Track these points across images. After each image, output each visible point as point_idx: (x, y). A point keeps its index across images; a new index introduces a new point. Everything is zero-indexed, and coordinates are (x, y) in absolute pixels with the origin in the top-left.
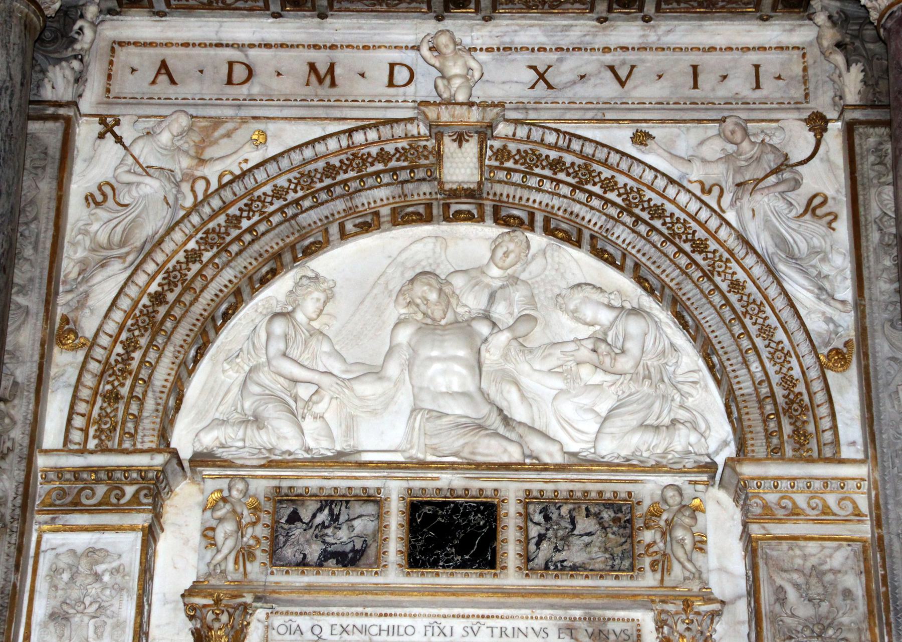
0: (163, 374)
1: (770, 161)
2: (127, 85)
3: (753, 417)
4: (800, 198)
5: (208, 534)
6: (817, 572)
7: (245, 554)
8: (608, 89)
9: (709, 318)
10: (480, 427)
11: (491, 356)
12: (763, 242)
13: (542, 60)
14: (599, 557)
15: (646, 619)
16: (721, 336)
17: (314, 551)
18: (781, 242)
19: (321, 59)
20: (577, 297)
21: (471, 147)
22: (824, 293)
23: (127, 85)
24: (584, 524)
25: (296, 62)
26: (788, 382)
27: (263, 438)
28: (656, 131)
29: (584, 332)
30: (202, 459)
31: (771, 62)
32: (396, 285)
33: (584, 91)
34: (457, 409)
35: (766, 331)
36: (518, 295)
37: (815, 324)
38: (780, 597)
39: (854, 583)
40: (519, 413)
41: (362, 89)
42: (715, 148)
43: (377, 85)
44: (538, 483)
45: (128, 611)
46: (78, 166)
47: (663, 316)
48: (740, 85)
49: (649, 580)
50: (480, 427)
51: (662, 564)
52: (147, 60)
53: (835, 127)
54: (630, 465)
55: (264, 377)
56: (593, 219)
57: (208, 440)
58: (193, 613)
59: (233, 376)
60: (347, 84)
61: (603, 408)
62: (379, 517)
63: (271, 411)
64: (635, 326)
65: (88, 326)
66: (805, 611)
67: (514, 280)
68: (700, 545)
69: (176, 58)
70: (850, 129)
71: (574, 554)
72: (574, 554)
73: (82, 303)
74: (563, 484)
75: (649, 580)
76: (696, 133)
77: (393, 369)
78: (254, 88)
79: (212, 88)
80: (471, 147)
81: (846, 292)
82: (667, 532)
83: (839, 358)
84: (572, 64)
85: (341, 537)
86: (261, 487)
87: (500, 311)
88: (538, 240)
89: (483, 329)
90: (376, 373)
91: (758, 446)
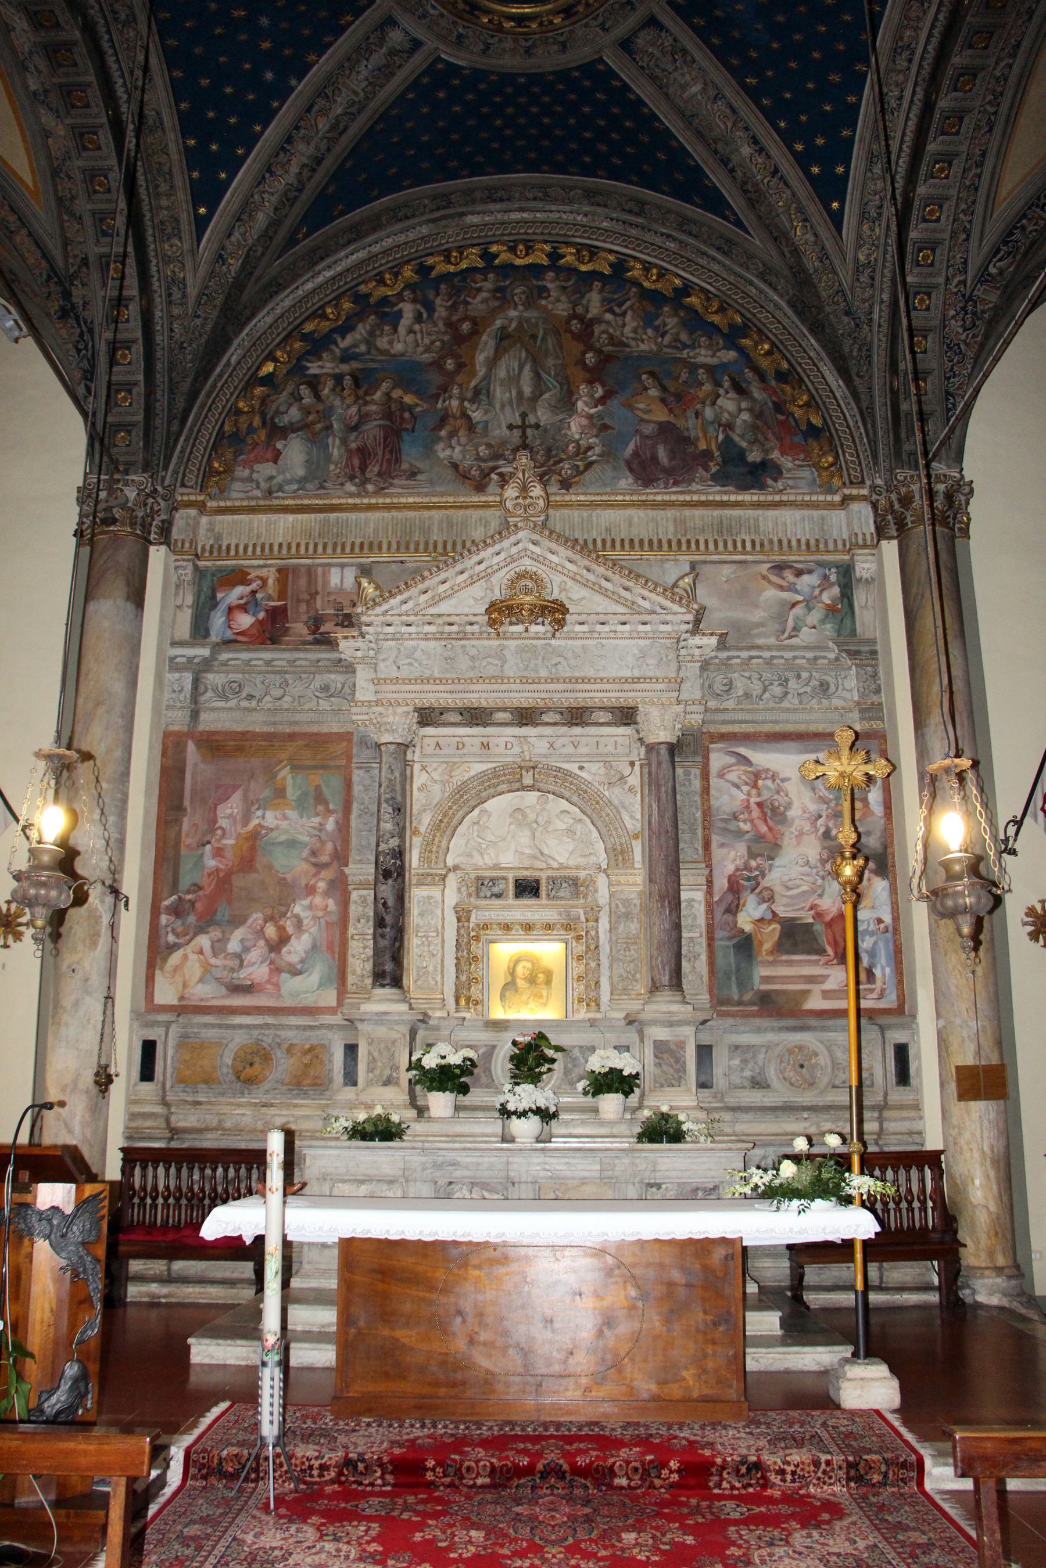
0: (444, 845)
1: (618, 777)
2: (428, 750)
3: (612, 855)
4: (627, 787)
5: (459, 889)
6: (627, 900)
7: (470, 895)
8: (571, 749)
9: (599, 824)
10: (535, 857)
11: (537, 834)
12: (616, 802)
13: (551, 740)
14: (568, 895)
15: (581, 911)
16: (603, 830)
17: (489, 894)
18: (621, 802)
19: (485, 740)
20: (562, 816)
21: (531, 773)
22: (632, 817)
23: (428, 750)
24: (564, 885)
25: (477, 741)
26: (621, 844)
27: (474, 861)
28: (585, 765)
29: (564, 826)
30: (456, 868)
31: (620, 740)
32: (510, 811)
33: (565, 751)
34: (528, 851)
35: (616, 829)
36: (545, 814)
37: (629, 827)
38: (617, 906)
39: (637, 902)
40: (546, 851)
41: (498, 750)
42: (603, 771)
43: (501, 750)
44: (550, 873)
45: (439, 913)
46: (415, 779)
47: (588, 821)
48: (610, 748)
49: (582, 901)
50: (535, 857)
51: (585, 897)
52: (432, 742)
53: (637, 763)
54: (577, 868)
55: (472, 842)
56: (567, 794)
57: (457, 861)
58: (457, 912)
59: (463, 841)
60: (493, 749)
61: (571, 849)
62: (507, 883)
63: (475, 853)
64: (579, 826)
65: (422, 829)
66: (623, 910)
67: (544, 809)
68: (596, 891)
69: (441, 741)
70: (641, 766)
71: (561, 894)
72: (561, 894)
73: (419, 823)
74: (557, 874)
75: (582, 901)
76: (598, 765)
77: (509, 838)
78: (465, 751)
79: (452, 751)
80: (531, 773)
81: (639, 817)
82: (587, 887)
83: (636, 837)
84: (560, 741)
85: (496, 890)
86: (473, 876)
87: (540, 819)
88: (551, 796)
89: (535, 825)
90: (504, 839)
91: (613, 863)
